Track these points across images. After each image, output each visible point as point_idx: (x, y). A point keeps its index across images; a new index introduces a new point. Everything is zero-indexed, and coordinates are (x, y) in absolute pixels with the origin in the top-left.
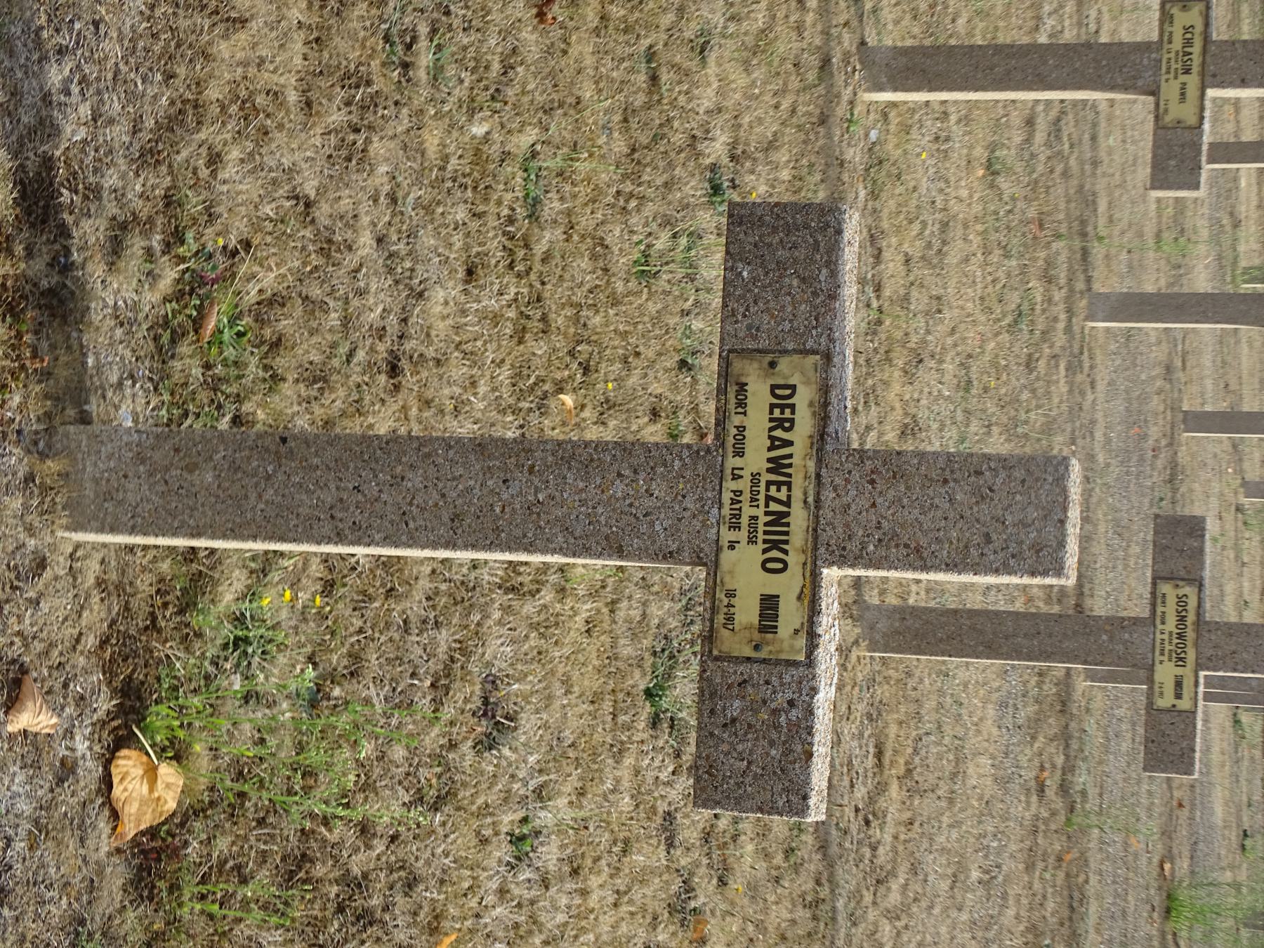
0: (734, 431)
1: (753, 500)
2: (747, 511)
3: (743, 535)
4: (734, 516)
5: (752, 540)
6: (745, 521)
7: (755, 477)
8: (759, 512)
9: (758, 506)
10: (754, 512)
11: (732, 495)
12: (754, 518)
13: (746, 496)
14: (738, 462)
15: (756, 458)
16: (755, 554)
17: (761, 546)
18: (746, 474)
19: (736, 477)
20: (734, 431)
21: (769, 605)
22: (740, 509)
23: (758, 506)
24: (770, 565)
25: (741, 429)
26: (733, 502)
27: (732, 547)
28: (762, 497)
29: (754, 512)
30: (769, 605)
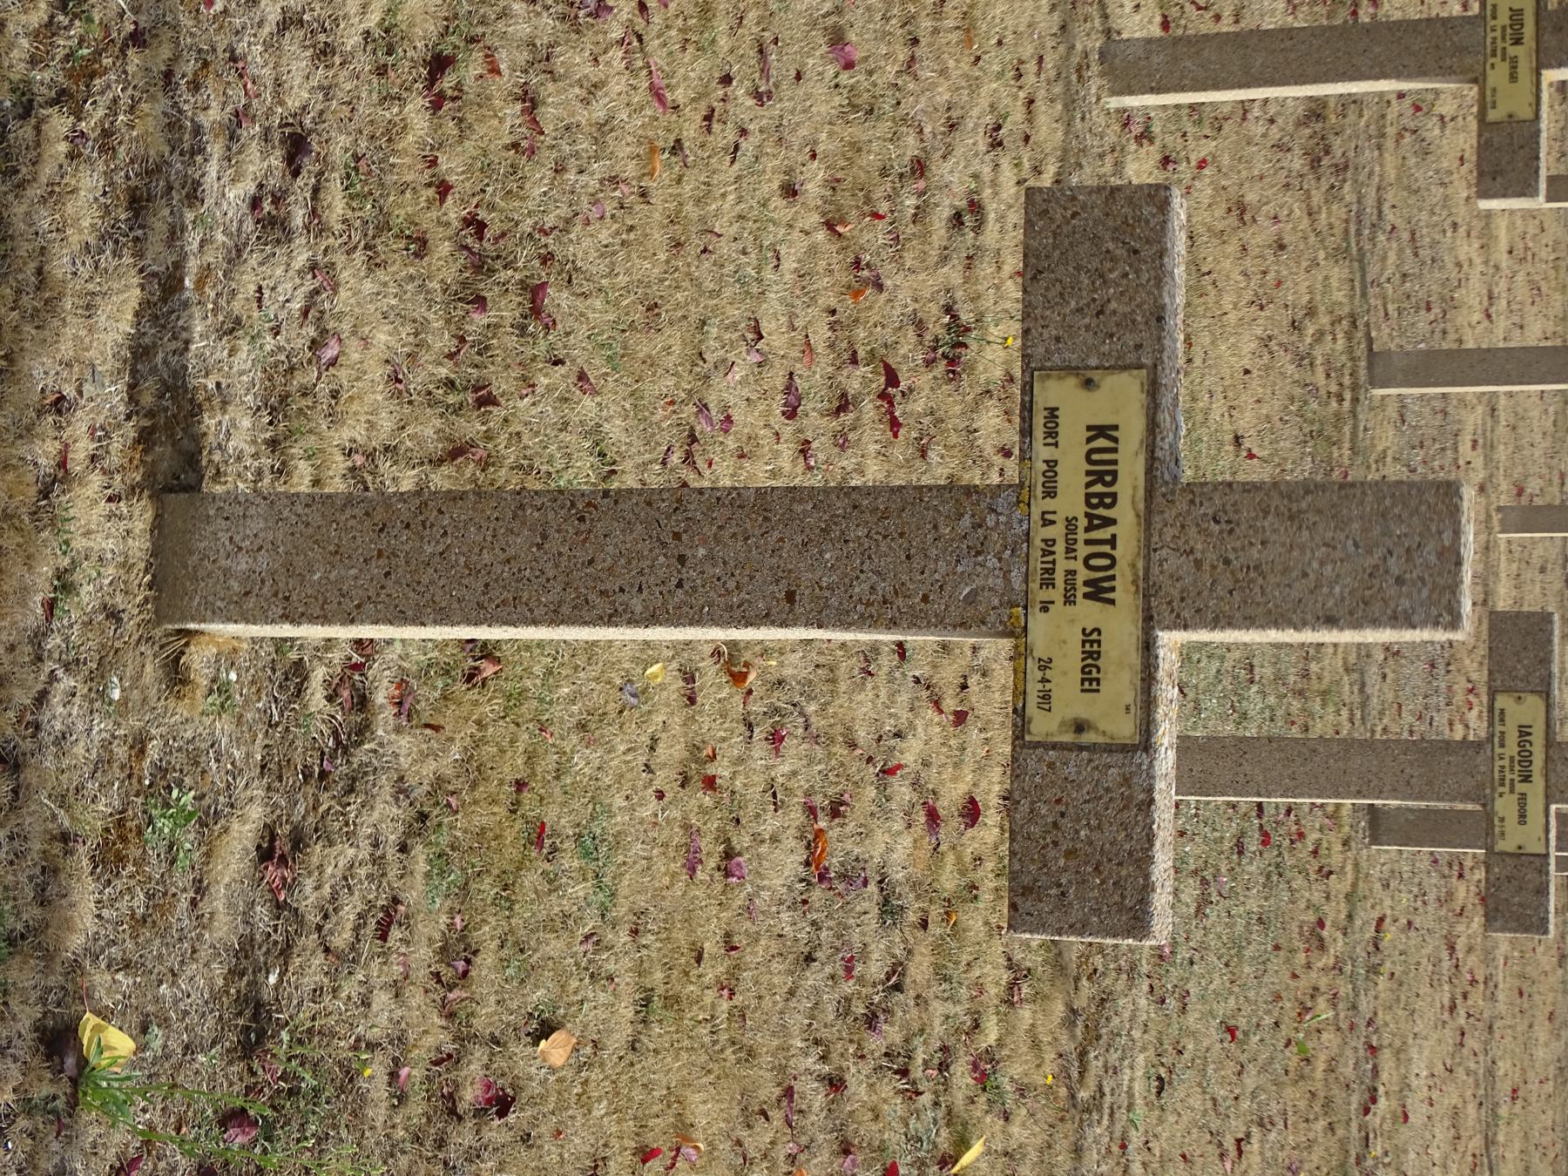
0: (1045, 467)
1: (1068, 550)
2: (1062, 565)
3: (1057, 594)
4: (1046, 571)
5: (1069, 600)
6: (1059, 577)
7: (1071, 523)
8: (1078, 565)
10: (1072, 565)
11: (1043, 545)
12: (1072, 573)
13: (1060, 548)
14: (1049, 504)
15: (1071, 501)
18: (1060, 518)
19: (1047, 523)
22: (1054, 562)
25: (1052, 464)
26: (1045, 553)
27: (1045, 609)
29: (1072, 565)
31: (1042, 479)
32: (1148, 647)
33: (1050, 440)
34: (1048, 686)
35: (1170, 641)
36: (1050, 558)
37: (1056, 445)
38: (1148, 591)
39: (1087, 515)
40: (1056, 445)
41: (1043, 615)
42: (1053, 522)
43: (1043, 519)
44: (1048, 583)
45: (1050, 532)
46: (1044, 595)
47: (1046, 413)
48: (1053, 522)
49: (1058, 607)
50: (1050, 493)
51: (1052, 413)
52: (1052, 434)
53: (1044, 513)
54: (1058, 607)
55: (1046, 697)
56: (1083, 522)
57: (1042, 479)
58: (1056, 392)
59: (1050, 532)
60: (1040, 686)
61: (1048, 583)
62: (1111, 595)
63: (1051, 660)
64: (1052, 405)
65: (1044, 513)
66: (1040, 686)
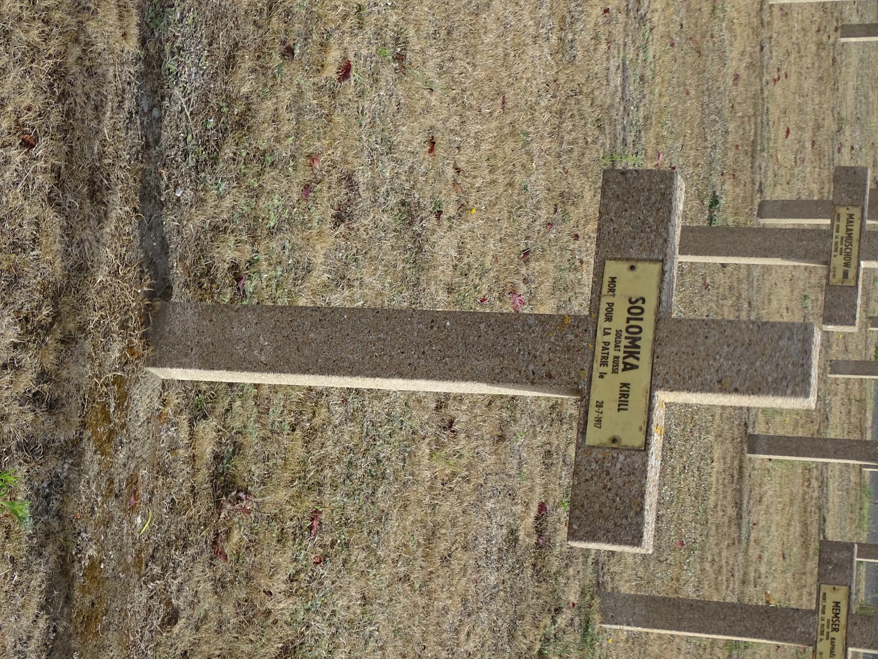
0: (607, 306)
1: (616, 346)
2: (612, 353)
3: (608, 369)
5: (615, 371)
8: (621, 355)
9: (619, 350)
11: (603, 345)
12: (617, 357)
13: (612, 347)
14: (607, 325)
19: (606, 334)
20: (607, 306)
23: (619, 350)
27: (602, 376)
29: (617, 354)
32: (651, 398)
33: (611, 293)
35: (663, 397)
36: (606, 351)
37: (614, 296)
42: (609, 334)
44: (604, 363)
45: (606, 338)
46: (603, 369)
47: (610, 280)
48: (609, 334)
49: (610, 376)
50: (609, 319)
51: (613, 280)
52: (612, 290)
53: (605, 329)
54: (610, 376)
55: (599, 421)
59: (606, 338)
61: (604, 363)
63: (603, 402)
65: (605, 329)
66: (596, 414)
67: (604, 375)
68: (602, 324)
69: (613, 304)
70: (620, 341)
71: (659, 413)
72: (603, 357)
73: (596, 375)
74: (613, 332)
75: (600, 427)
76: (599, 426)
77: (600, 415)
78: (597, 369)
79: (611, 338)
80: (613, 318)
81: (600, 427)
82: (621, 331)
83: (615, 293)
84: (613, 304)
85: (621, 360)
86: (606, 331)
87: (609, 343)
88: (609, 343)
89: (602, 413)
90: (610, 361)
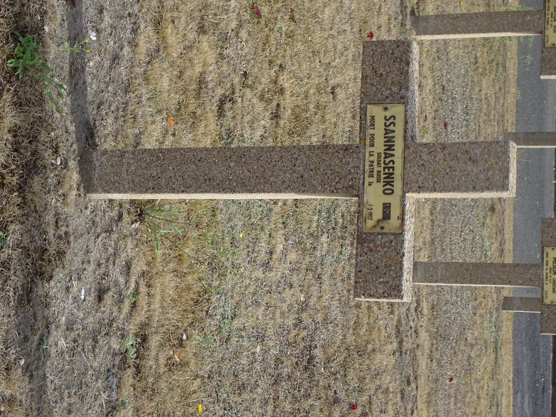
0: (370, 136)
1: (378, 164)
2: (376, 169)
3: (374, 179)
4: (371, 172)
5: (379, 181)
6: (375, 174)
7: (379, 155)
8: (381, 169)
9: (380, 166)
11: (370, 163)
12: (379, 172)
13: (375, 164)
14: (372, 149)
15: (380, 146)
16: (379, 187)
17: (383, 184)
19: (371, 155)
20: (370, 136)
21: (387, 207)
22: (373, 169)
23: (380, 166)
24: (386, 192)
25: (373, 135)
26: (370, 166)
27: (370, 184)
28: (382, 162)
29: (379, 169)
30: (387, 207)
31: (369, 140)
33: (372, 127)
34: (371, 211)
35: (411, 197)
36: (372, 167)
37: (374, 129)
38: (405, 184)
39: (384, 153)
40: (374, 129)
41: (369, 187)
43: (370, 154)
44: (371, 176)
45: (372, 159)
46: (371, 180)
47: (370, 118)
48: (373, 155)
50: (372, 145)
51: (373, 118)
52: (373, 125)
53: (370, 152)
56: (383, 156)
57: (369, 140)
58: (375, 111)
60: (369, 211)
62: (393, 148)
64: (373, 115)
65: (370, 152)
66: (369, 211)
67: (372, 184)
68: (369, 149)
69: (374, 134)
70: (381, 160)
71: (409, 207)
72: (371, 172)
73: (366, 184)
74: (376, 154)
75: (372, 219)
76: (371, 218)
77: (371, 211)
78: (367, 180)
79: (374, 158)
80: (375, 144)
81: (372, 219)
82: (381, 153)
83: (375, 126)
84: (374, 134)
85: (382, 172)
86: (371, 153)
87: (373, 161)
88: (373, 161)
89: (372, 209)
90: (375, 174)
